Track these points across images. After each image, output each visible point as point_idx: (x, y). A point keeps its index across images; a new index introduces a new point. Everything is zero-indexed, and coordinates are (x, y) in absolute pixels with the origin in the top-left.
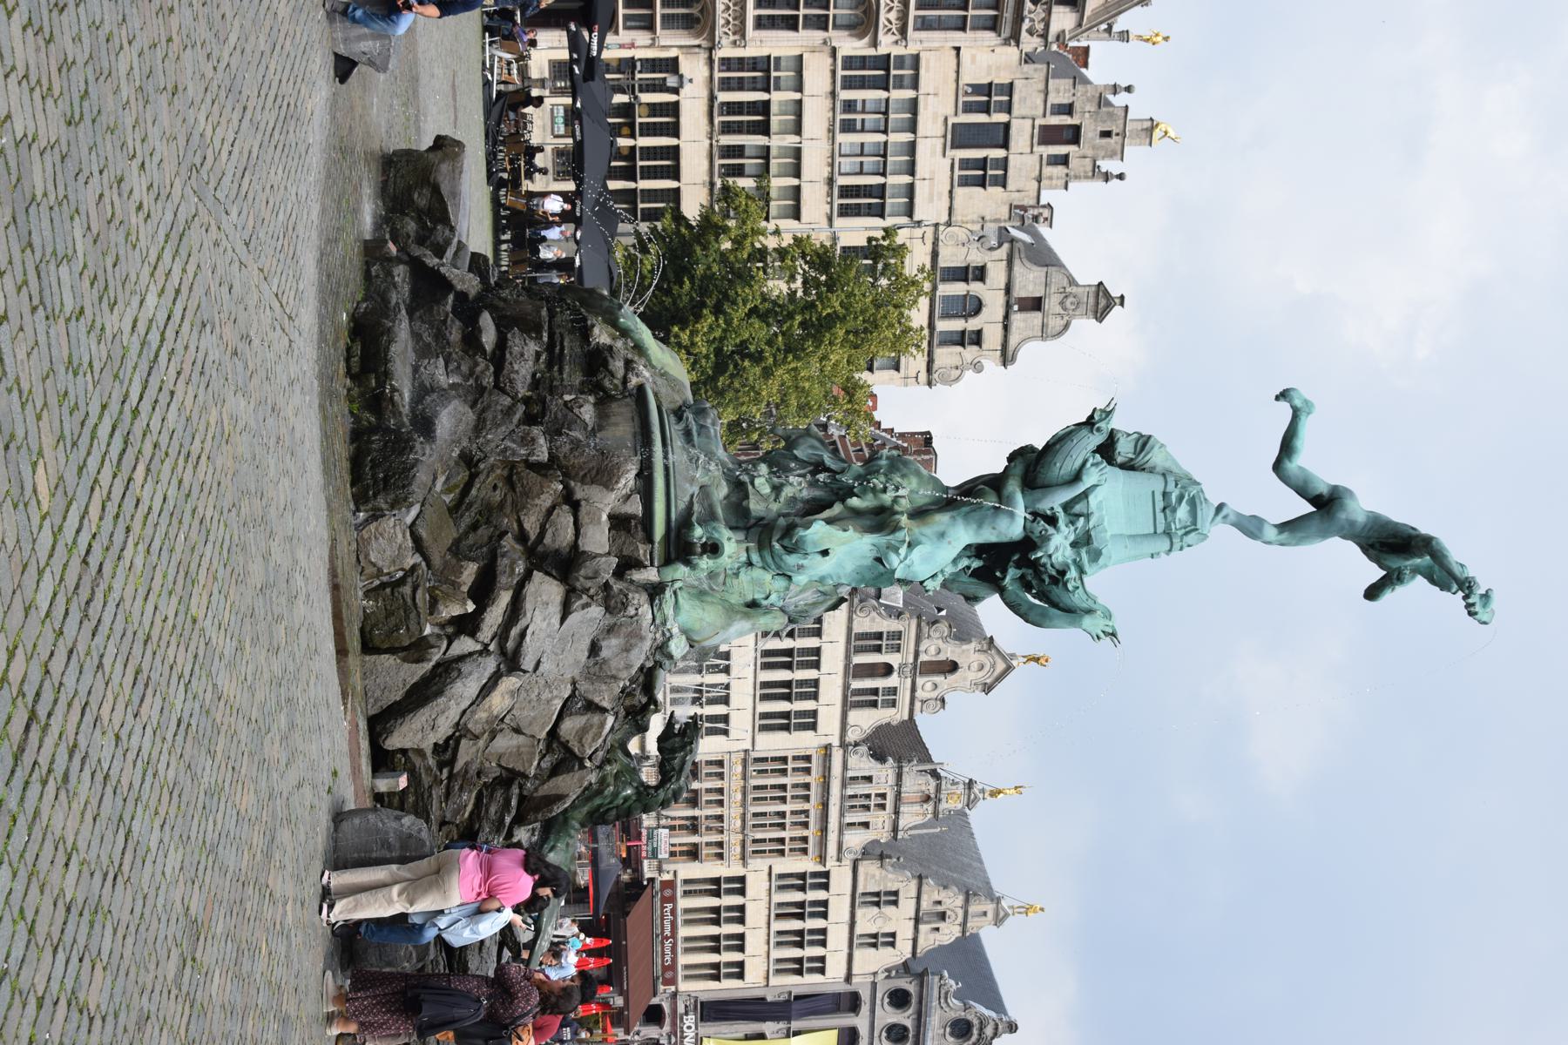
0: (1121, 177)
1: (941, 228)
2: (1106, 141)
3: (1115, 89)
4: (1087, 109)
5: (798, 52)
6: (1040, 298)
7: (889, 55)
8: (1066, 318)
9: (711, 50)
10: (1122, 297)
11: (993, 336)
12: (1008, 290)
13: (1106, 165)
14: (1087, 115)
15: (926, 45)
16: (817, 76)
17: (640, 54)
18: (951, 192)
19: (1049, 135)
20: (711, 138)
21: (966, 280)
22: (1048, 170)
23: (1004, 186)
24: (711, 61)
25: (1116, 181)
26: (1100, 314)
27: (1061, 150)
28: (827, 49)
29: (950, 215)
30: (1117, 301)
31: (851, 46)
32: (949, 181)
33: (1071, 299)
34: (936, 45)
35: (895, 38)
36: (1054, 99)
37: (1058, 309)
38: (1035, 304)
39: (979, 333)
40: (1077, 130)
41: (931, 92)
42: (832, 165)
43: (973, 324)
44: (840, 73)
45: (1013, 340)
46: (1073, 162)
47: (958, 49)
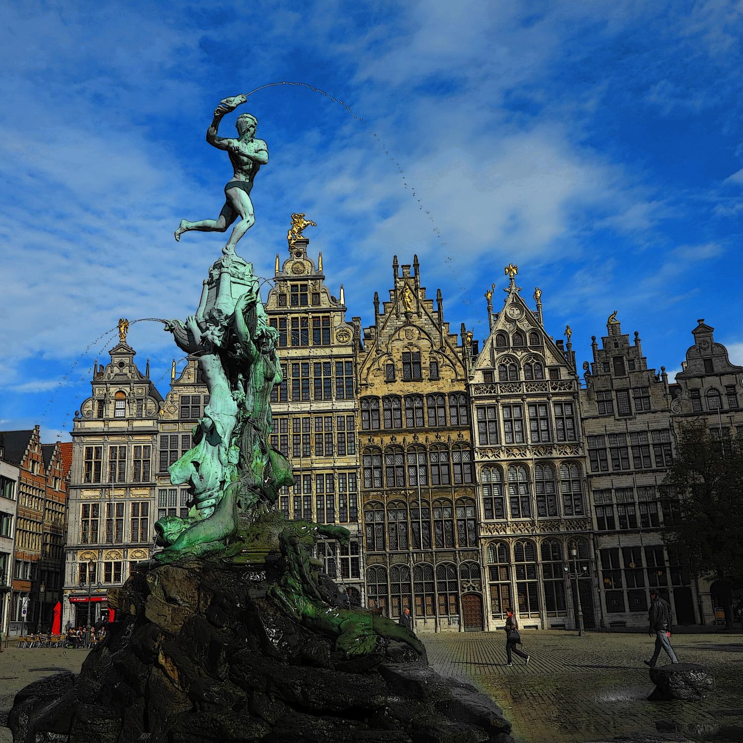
0: (636, 334)
1: (672, 414)
2: (619, 345)
3: (594, 345)
4: (605, 356)
5: (592, 493)
6: (704, 360)
7: (589, 450)
8: (713, 346)
9: (595, 534)
10: (699, 321)
11: (727, 380)
12: (701, 377)
13: (632, 344)
14: (608, 355)
15: (581, 434)
16: (603, 483)
17: (600, 568)
18: (653, 413)
19: (620, 371)
20: (639, 532)
21: (699, 398)
22: (637, 369)
23: (648, 387)
24: (600, 535)
25: (639, 337)
26: (710, 330)
27: (626, 363)
28: (589, 479)
29: (665, 411)
30: (701, 323)
31: (587, 467)
32: (648, 414)
33: (703, 346)
34: (580, 429)
35: (580, 449)
36: (601, 371)
37: (709, 351)
38: (708, 362)
39: (727, 387)
40: (615, 358)
41: (604, 428)
42: (646, 472)
43: (723, 391)
44: (600, 473)
45: (730, 370)
46: (632, 356)
47: (582, 420)
